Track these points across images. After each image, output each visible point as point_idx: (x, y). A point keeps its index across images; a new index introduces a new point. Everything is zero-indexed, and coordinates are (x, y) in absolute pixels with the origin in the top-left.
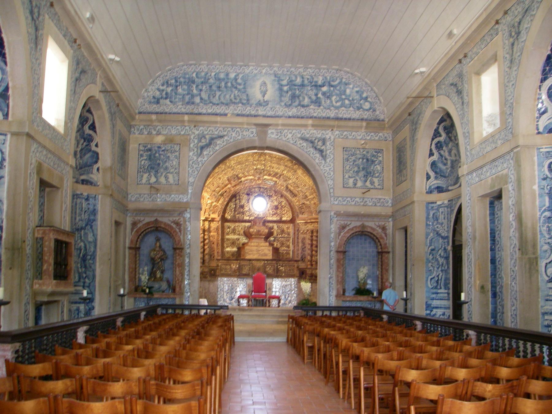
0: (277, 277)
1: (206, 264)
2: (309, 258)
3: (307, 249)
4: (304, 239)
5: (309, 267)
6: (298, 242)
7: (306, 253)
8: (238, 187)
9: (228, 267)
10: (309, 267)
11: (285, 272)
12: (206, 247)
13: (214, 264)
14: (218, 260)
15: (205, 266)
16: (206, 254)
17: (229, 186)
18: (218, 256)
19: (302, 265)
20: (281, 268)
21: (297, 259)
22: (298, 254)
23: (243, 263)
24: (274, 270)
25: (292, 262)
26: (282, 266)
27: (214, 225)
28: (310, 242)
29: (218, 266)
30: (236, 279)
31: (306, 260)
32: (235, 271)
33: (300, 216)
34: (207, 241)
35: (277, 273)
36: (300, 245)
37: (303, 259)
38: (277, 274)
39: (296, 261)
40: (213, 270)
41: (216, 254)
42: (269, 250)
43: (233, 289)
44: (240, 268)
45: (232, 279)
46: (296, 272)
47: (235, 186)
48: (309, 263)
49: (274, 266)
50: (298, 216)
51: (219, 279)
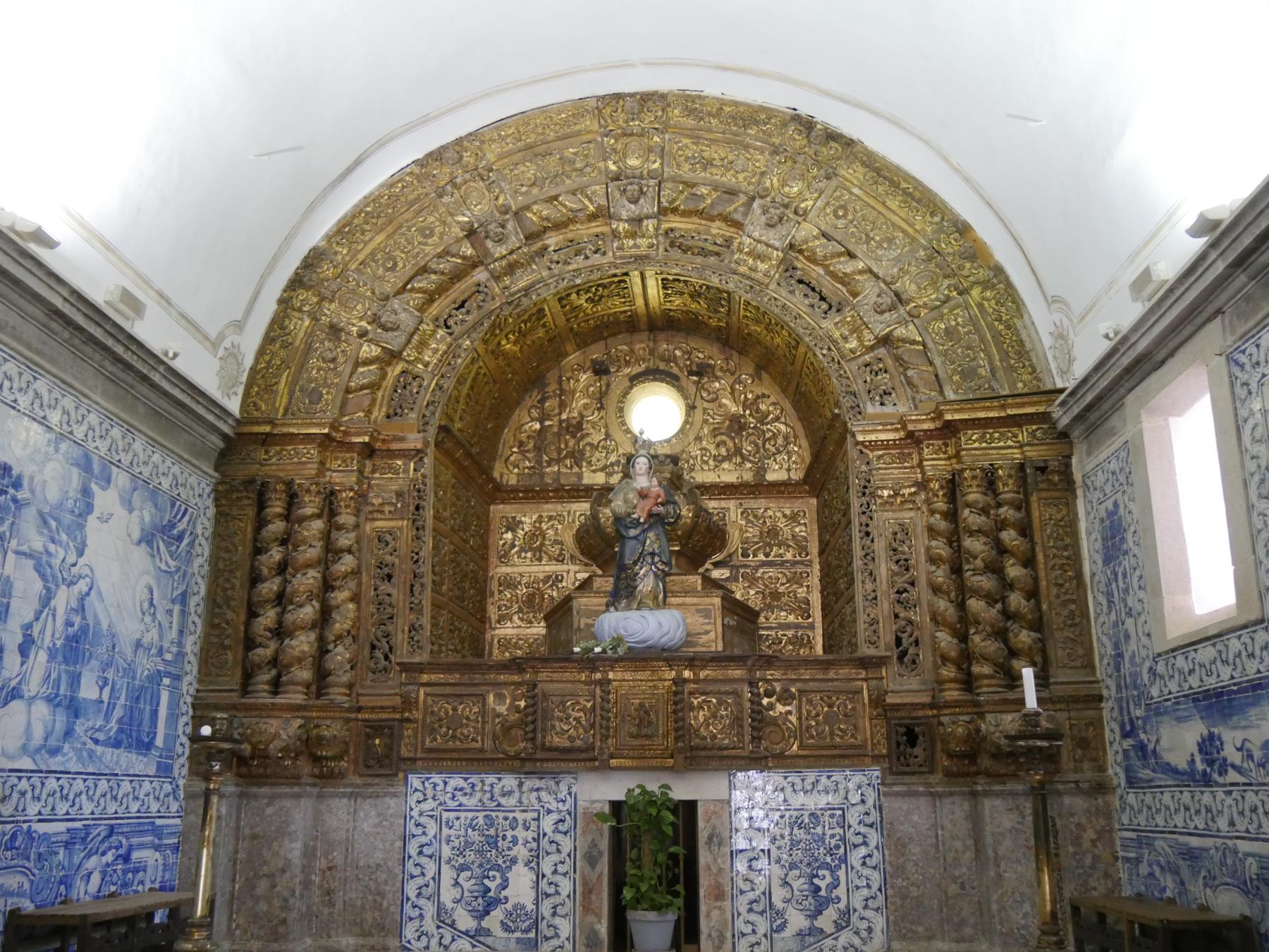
0: (758, 761)
1: (338, 695)
2: (945, 639)
3: (922, 592)
4: (903, 533)
5: (952, 694)
6: (869, 556)
7: (920, 616)
8: (523, 280)
9: (469, 709)
10: (952, 694)
11: (801, 732)
12: (340, 596)
13: (383, 693)
14: (405, 667)
15: (333, 706)
16: (339, 638)
17: (480, 275)
18: (415, 646)
19: (905, 688)
20: (780, 708)
21: (871, 652)
22: (874, 622)
23: (552, 681)
24: (737, 721)
25: (844, 672)
26: (785, 698)
27: (391, 481)
28: (941, 548)
29: (408, 703)
30: (509, 781)
31: (925, 657)
32: (507, 729)
33: (871, 409)
34: (348, 562)
35: (756, 739)
36: (884, 568)
37: (903, 653)
38: (759, 748)
39: (865, 663)
40: (376, 728)
41: (401, 639)
42: (706, 614)
43: (493, 842)
44: (534, 718)
45: (490, 779)
46: (870, 730)
47: (511, 269)
48: (948, 672)
49: (737, 694)
50: (858, 410)
51: (414, 780)
